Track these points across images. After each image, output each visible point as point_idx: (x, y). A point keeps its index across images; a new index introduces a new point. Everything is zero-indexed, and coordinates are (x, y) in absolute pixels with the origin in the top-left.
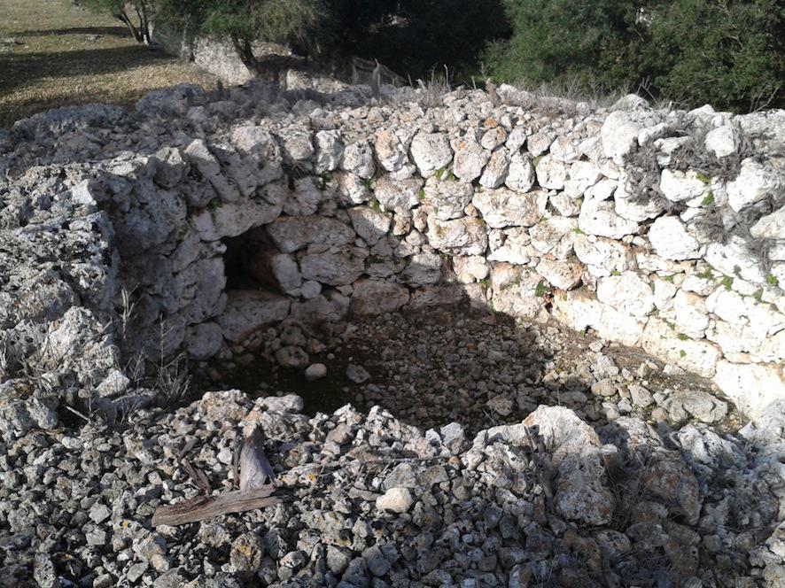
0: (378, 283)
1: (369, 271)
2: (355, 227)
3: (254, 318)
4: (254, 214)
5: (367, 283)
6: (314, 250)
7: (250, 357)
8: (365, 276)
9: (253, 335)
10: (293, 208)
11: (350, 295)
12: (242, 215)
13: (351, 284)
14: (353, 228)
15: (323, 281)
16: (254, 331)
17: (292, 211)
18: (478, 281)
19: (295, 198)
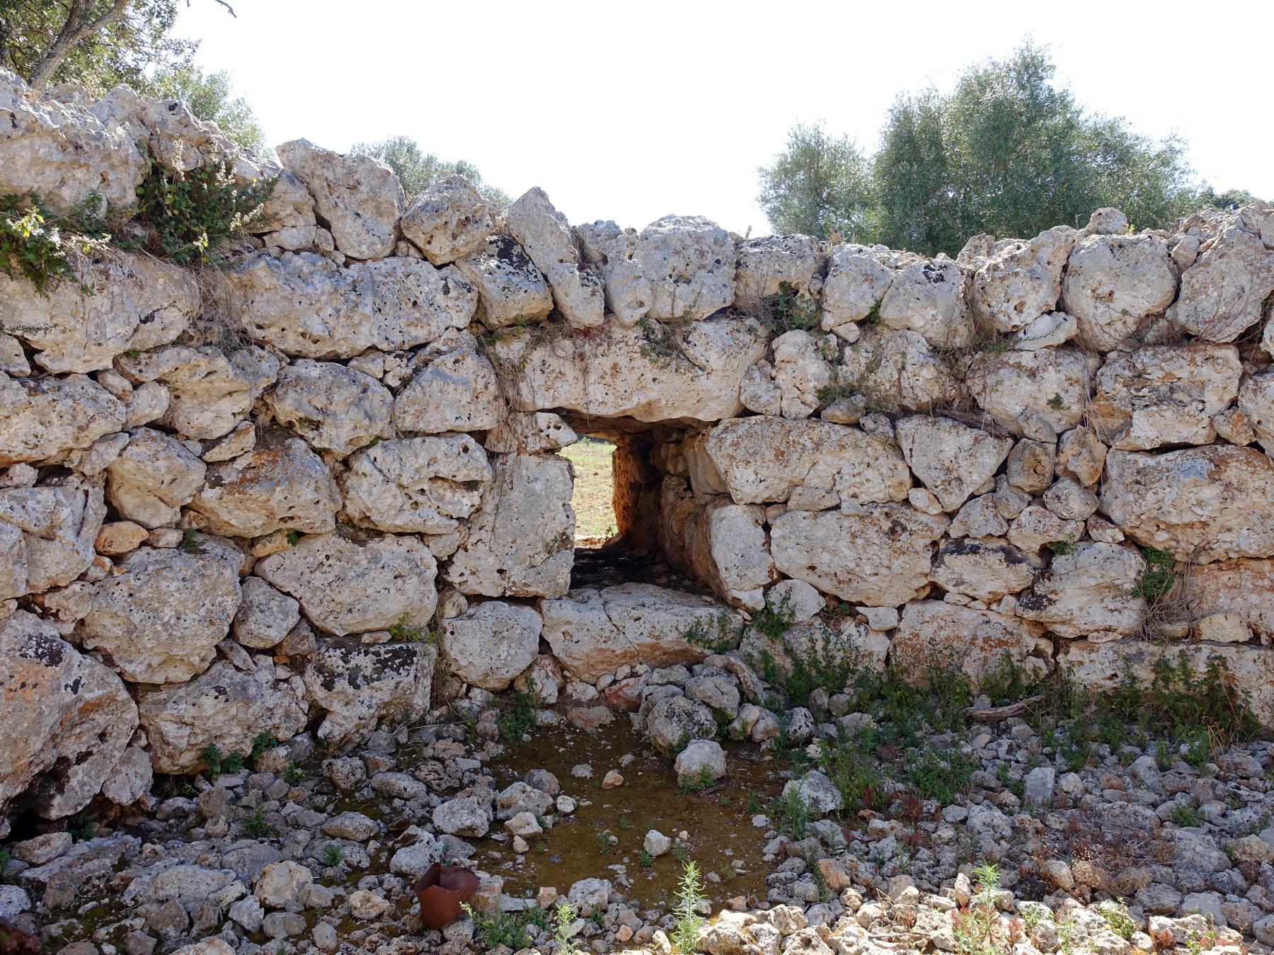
0: (965, 614)
1: (942, 577)
2: (907, 453)
3: (632, 630)
4: (649, 376)
5: (936, 607)
6: (802, 500)
7: (602, 714)
8: (937, 593)
9: (626, 670)
10: (760, 393)
11: (890, 633)
12: (615, 367)
13: (900, 608)
14: (903, 458)
15: (827, 586)
16: (629, 657)
17: (756, 398)
18: (1264, 640)
19: (773, 379)
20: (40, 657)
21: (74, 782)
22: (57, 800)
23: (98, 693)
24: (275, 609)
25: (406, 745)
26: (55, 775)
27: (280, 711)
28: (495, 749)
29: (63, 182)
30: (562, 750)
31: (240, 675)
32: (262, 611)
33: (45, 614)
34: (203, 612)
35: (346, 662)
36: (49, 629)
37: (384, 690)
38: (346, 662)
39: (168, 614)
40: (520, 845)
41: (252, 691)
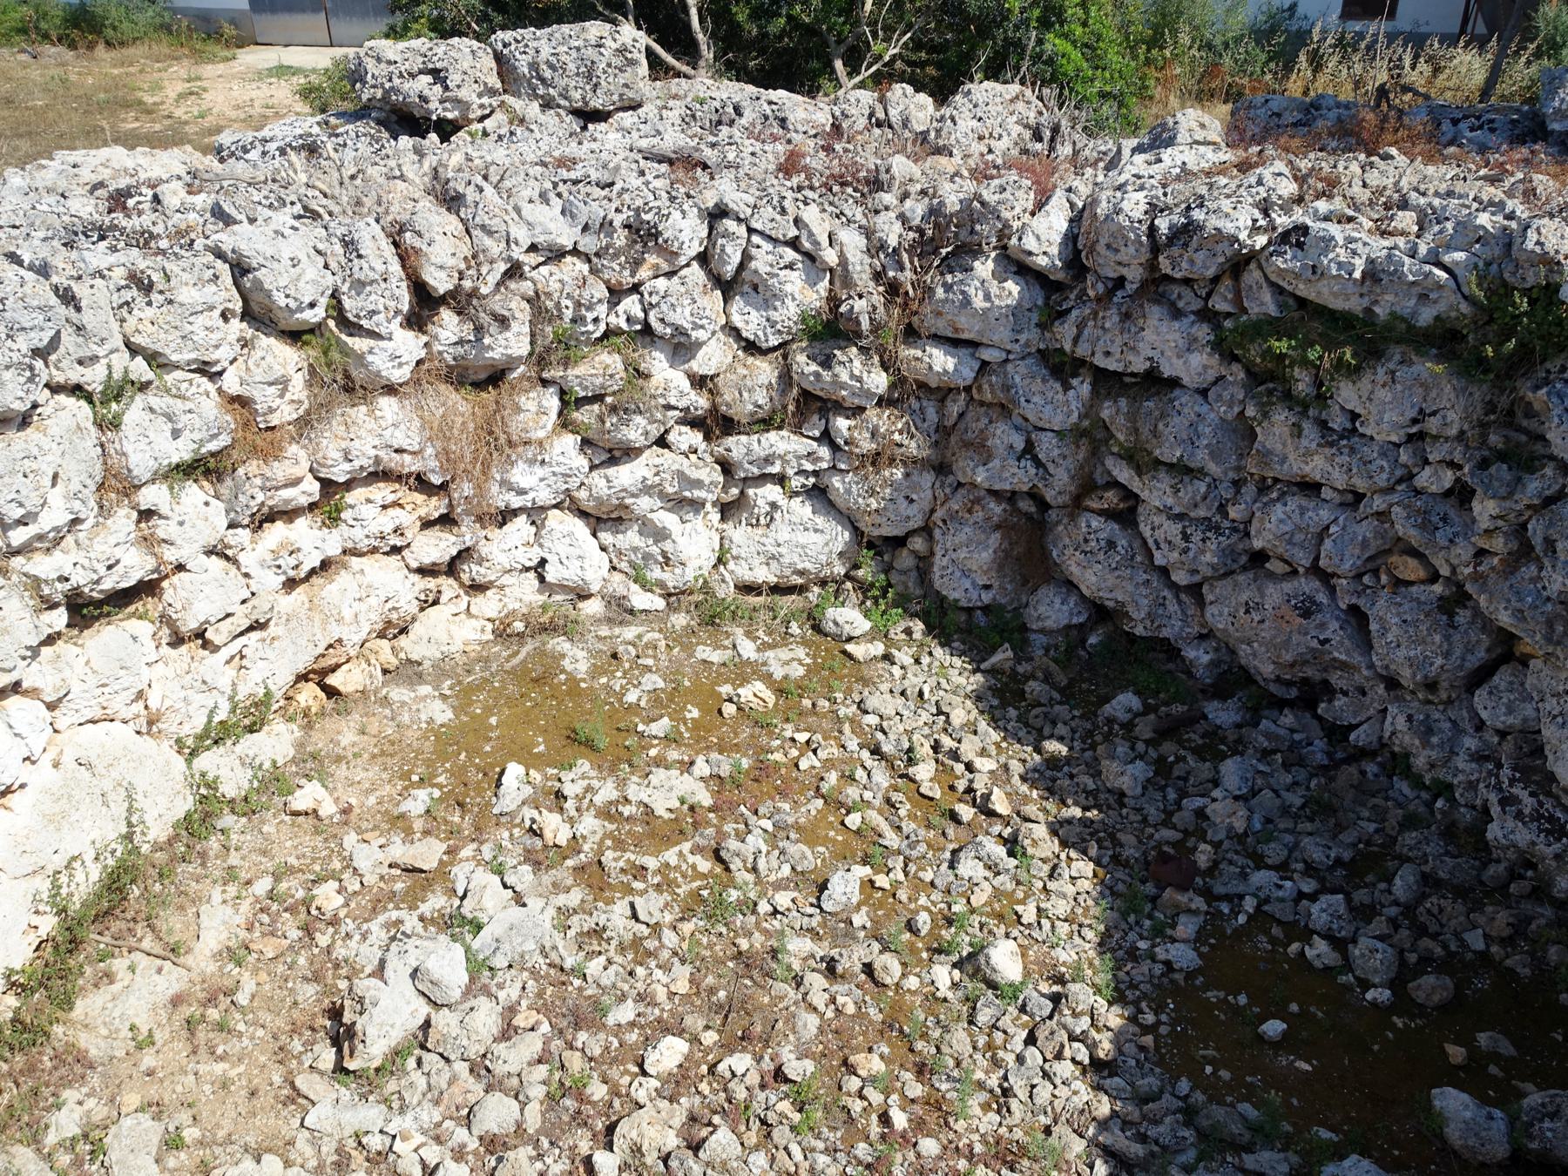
20: (1296, 607)
21: (1336, 703)
22: (1323, 705)
23: (1343, 657)
24: (1505, 700)
25: (1507, 895)
26: (1328, 690)
27: (1461, 777)
28: (1518, 962)
29: (1376, 302)
30: (1560, 1038)
31: (1448, 725)
32: (1490, 693)
33: (1332, 590)
34: (1412, 653)
35: (1511, 785)
36: (1322, 598)
37: (1523, 836)
38: (1511, 785)
39: (1390, 637)
40: (1295, 947)
41: (1435, 740)
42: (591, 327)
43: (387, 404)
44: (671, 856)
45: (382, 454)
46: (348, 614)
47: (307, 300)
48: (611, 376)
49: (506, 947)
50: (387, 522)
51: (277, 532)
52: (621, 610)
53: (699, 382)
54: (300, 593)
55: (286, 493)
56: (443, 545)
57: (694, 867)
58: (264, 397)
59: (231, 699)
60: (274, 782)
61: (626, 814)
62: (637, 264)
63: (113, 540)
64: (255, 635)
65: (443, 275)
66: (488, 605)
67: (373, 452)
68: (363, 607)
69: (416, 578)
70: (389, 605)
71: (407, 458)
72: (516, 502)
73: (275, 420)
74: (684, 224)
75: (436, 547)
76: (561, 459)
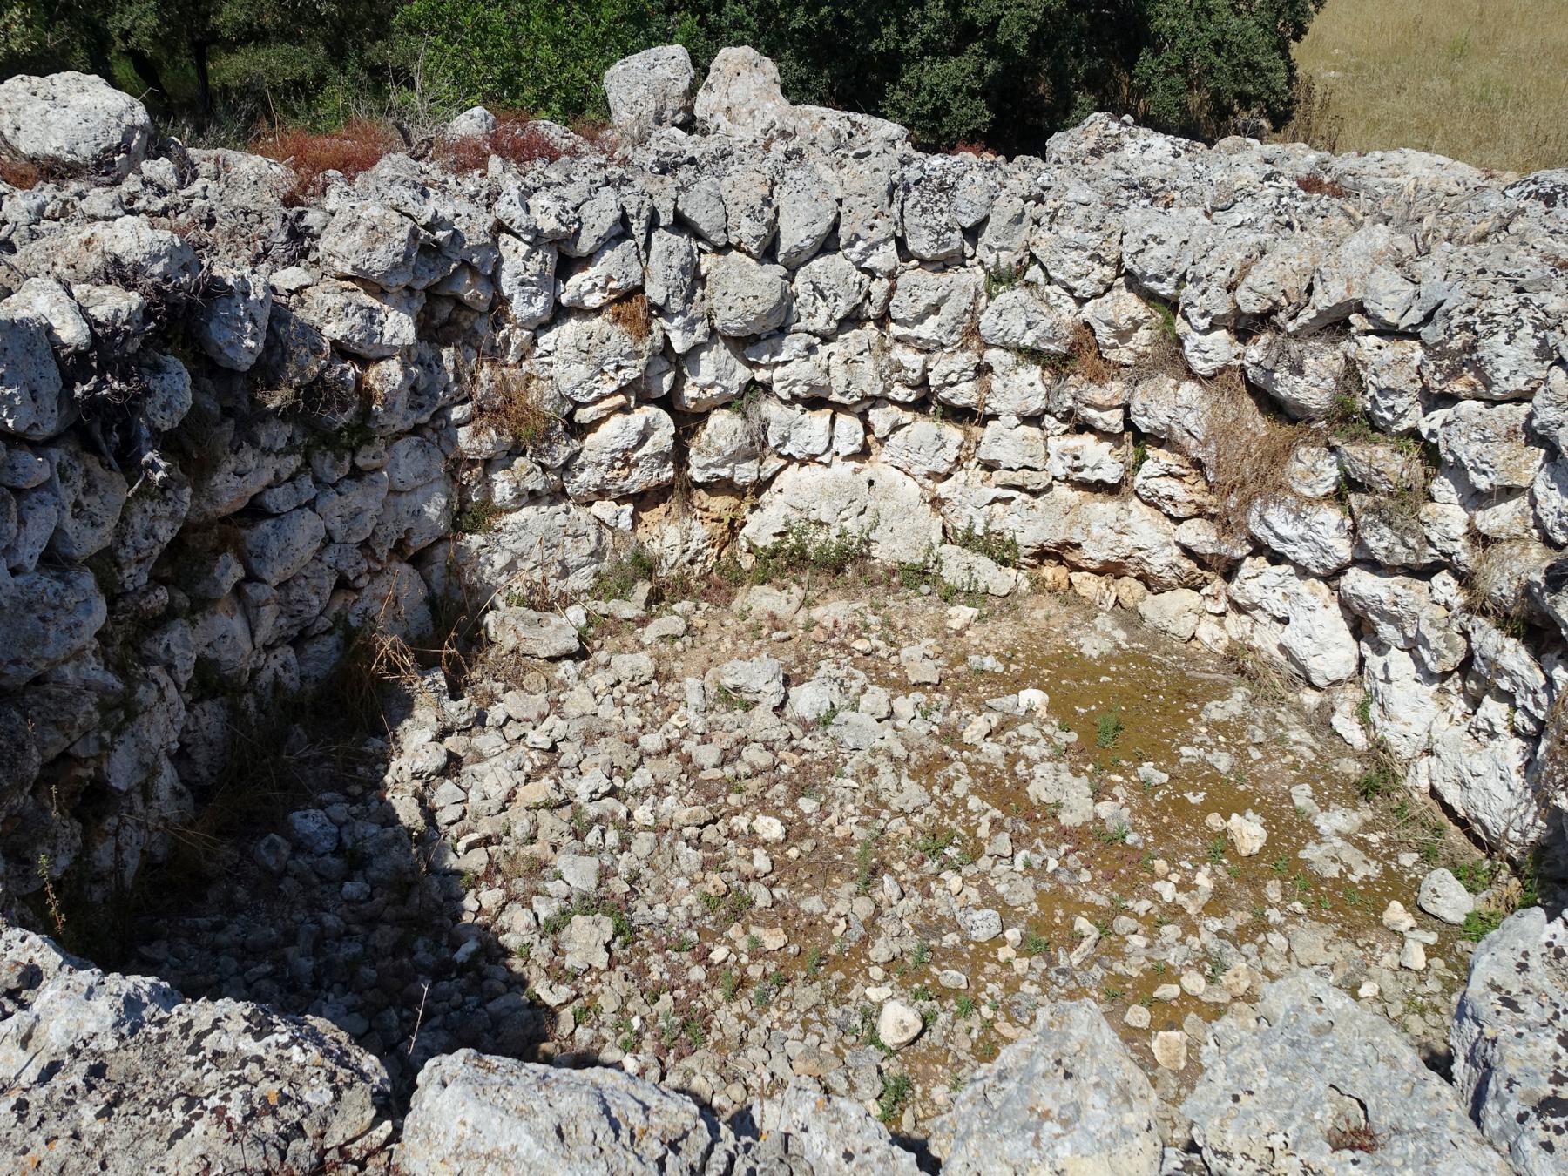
42: (1389, 416)
43: (1190, 389)
44: (974, 803)
45: (1175, 427)
46: (1096, 530)
47: (1150, 272)
48: (1379, 473)
49: (844, 729)
50: (1167, 487)
51: (1088, 439)
52: (1321, 722)
53: (1481, 540)
54: (1076, 496)
55: (1091, 413)
56: (1204, 538)
57: (979, 825)
58: (1104, 334)
59: (988, 524)
60: (973, 595)
61: (1017, 769)
62: (1454, 373)
63: (952, 367)
64: (1025, 496)
65: (1252, 296)
66: (1236, 626)
67: (1167, 420)
68: (1113, 536)
69: (1177, 551)
70: (1139, 554)
71: (1194, 442)
72: (1276, 545)
73: (1112, 355)
74: (1504, 350)
75: (1199, 535)
76: (1320, 528)
